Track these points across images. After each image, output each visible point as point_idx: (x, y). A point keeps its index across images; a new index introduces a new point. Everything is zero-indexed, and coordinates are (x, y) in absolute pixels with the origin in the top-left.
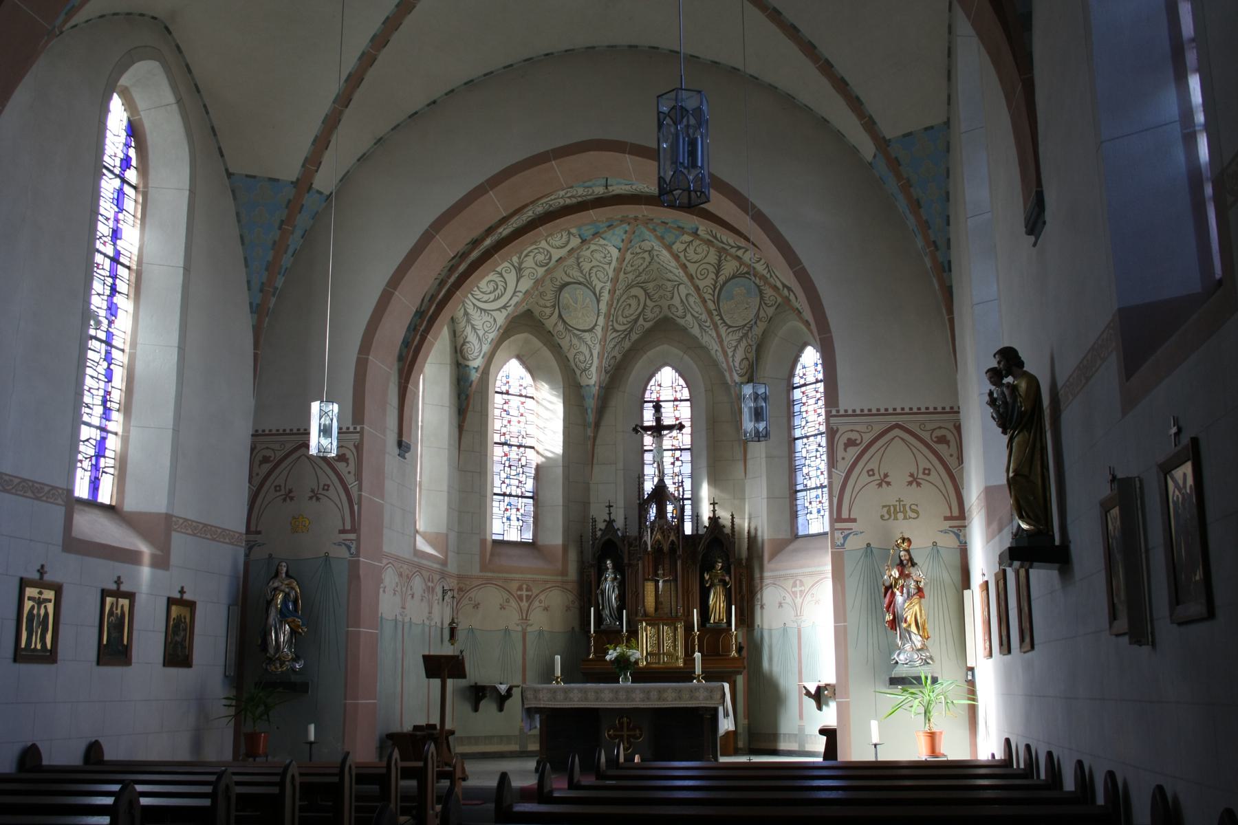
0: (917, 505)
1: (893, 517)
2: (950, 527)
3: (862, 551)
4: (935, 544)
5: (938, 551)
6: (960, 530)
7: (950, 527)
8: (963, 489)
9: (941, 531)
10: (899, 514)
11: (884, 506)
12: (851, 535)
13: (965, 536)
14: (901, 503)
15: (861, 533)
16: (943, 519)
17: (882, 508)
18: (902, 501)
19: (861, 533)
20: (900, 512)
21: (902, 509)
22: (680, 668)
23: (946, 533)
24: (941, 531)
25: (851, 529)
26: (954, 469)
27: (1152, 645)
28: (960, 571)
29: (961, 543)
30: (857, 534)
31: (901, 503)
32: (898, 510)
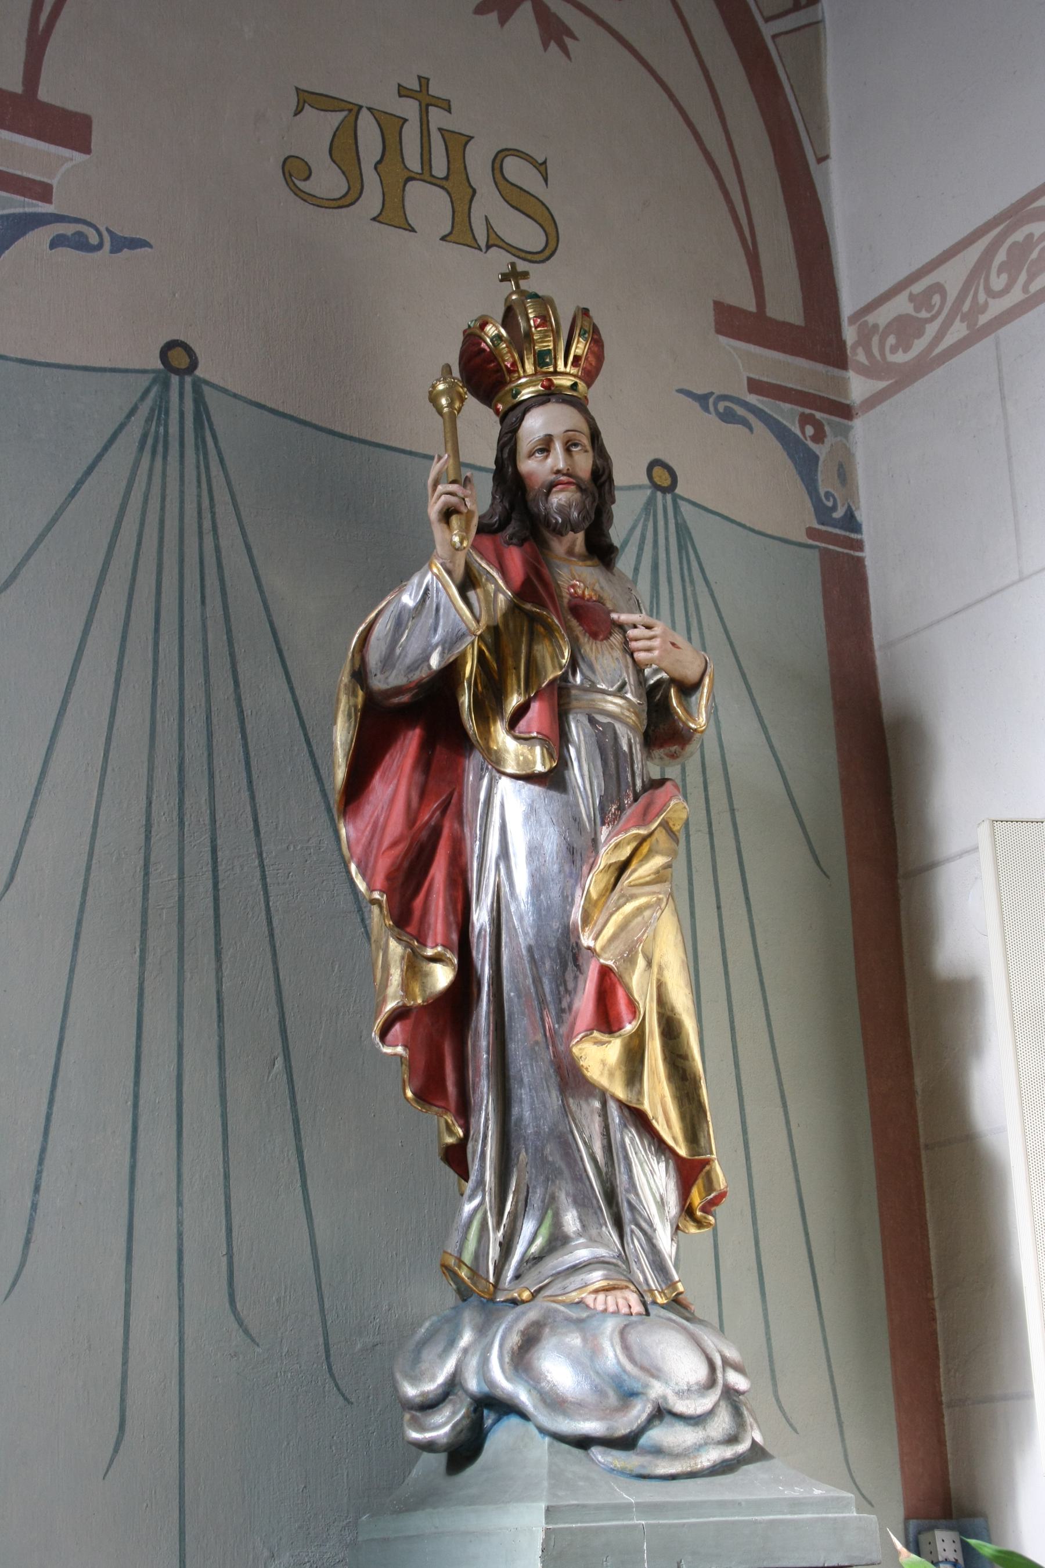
0: (542, 168)
1: (372, 200)
2: (755, 386)
3: (145, 381)
4: (662, 477)
5: (683, 532)
6: (818, 426)
7: (755, 386)
8: (822, 159)
9: (703, 400)
10: (415, 189)
11: (306, 99)
12: (42, 236)
13: (844, 474)
14: (437, 117)
15: (122, 244)
16: (709, 317)
17: (419, 77)
18: (446, 106)
19: (122, 244)
20: (426, 176)
21: (439, 169)
22: (401, 591)
23: (728, 417)
24: (703, 400)
25: (44, 192)
26: (767, 20)
27: (653, 1376)
28: (829, 718)
29: (823, 512)
30: (80, 243)
31: (437, 117)
32: (414, 164)
